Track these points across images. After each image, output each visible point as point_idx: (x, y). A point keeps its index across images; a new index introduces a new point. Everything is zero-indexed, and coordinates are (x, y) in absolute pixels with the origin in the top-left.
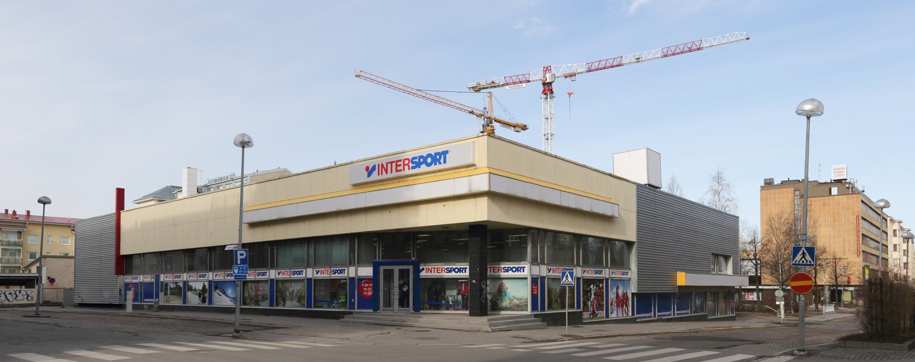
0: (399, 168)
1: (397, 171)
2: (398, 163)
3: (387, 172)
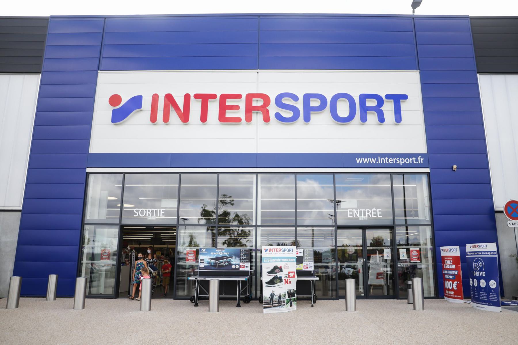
0: (229, 114)
1: (222, 118)
2: (229, 102)
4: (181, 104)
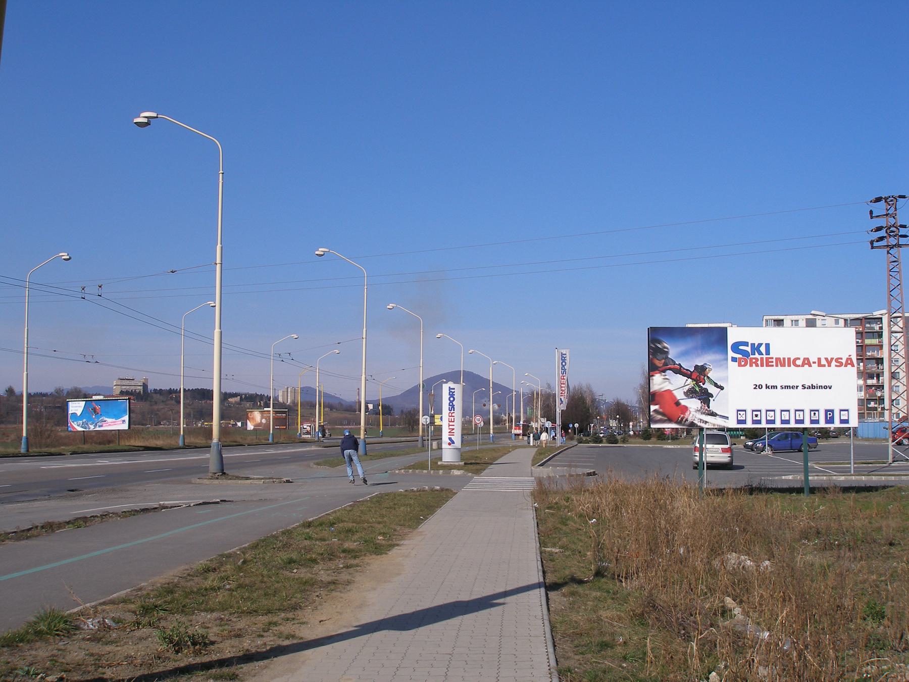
0: (453, 420)
1: (454, 422)
2: (450, 420)
3: (453, 429)
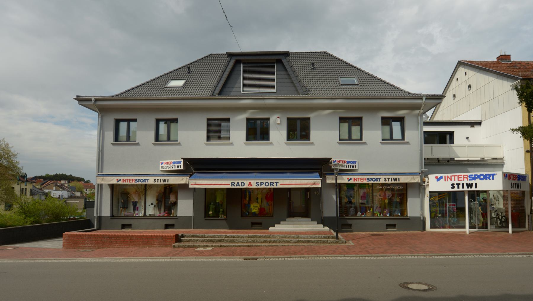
0: (460, 179)
1: (458, 180)
2: (459, 177)
3: (451, 180)
4: (450, 178)
